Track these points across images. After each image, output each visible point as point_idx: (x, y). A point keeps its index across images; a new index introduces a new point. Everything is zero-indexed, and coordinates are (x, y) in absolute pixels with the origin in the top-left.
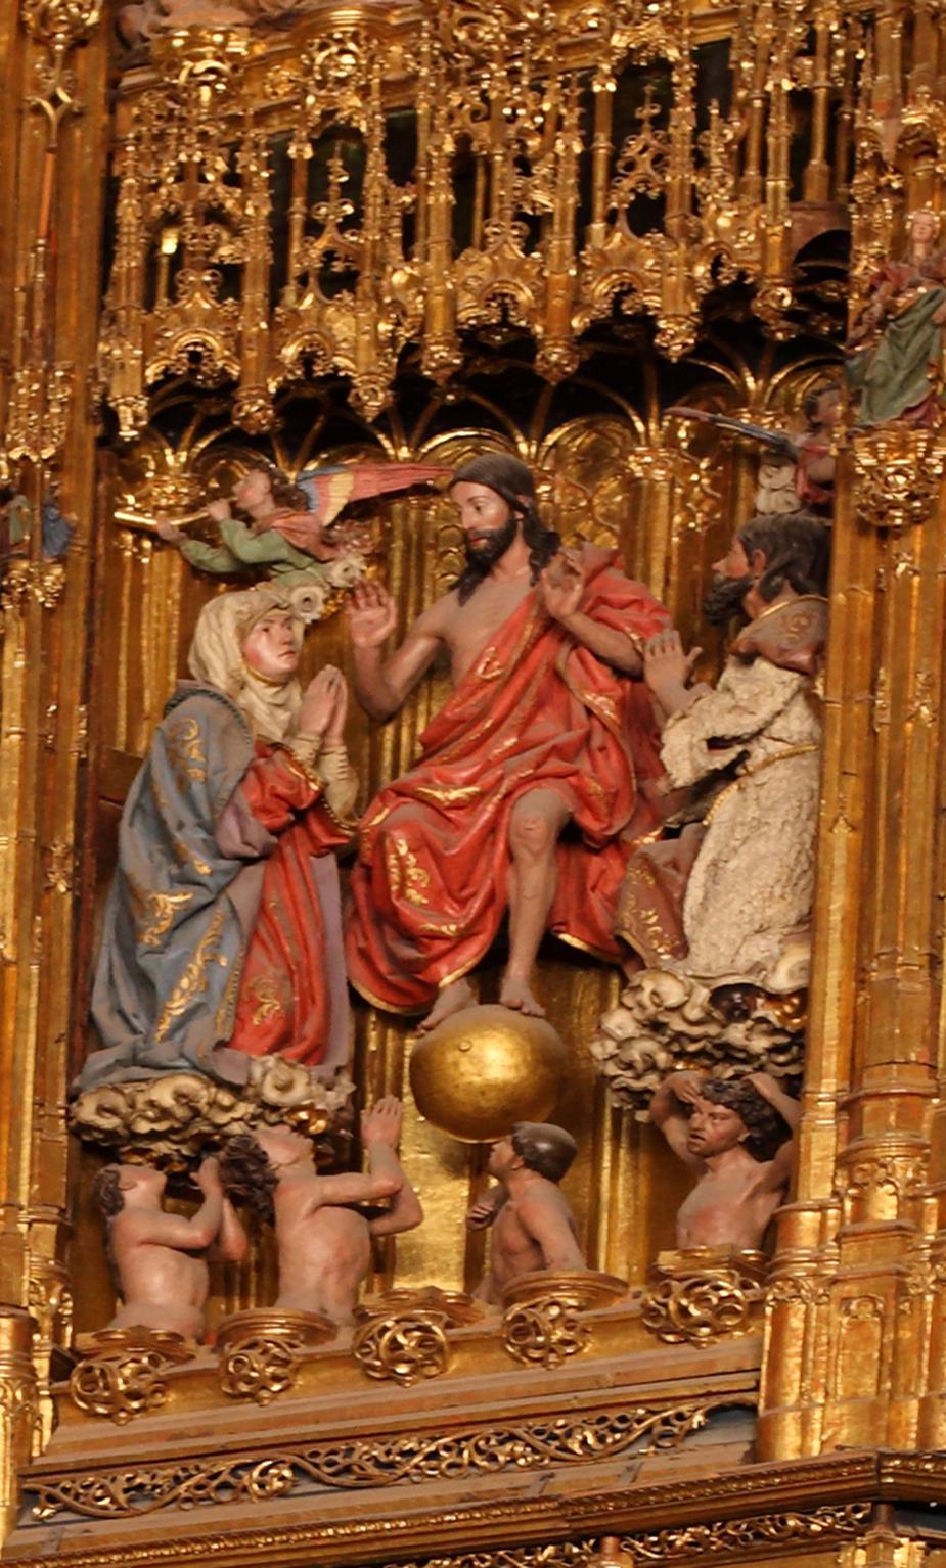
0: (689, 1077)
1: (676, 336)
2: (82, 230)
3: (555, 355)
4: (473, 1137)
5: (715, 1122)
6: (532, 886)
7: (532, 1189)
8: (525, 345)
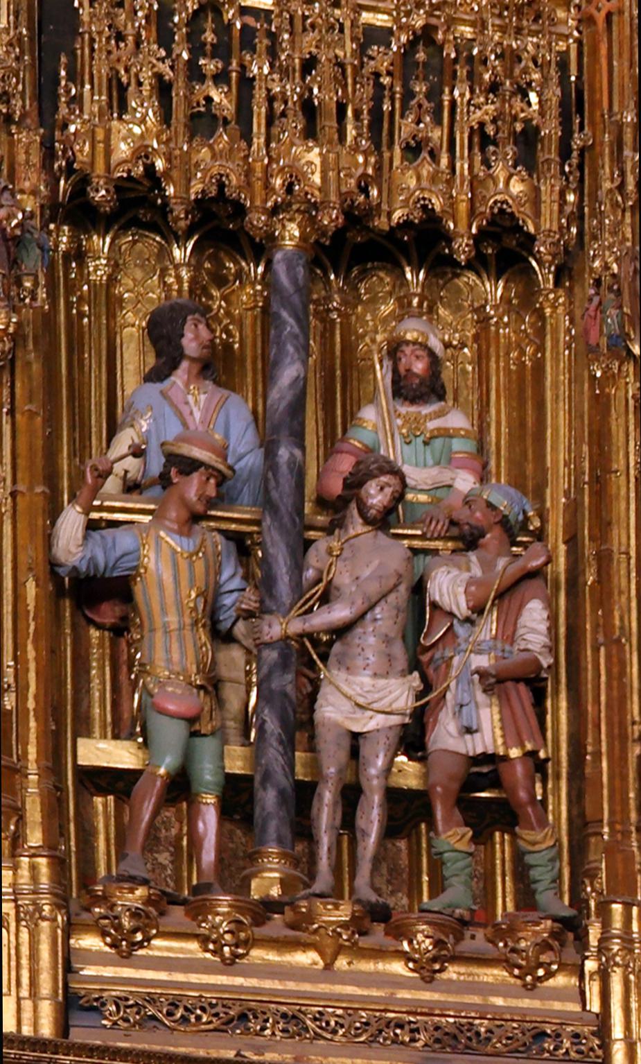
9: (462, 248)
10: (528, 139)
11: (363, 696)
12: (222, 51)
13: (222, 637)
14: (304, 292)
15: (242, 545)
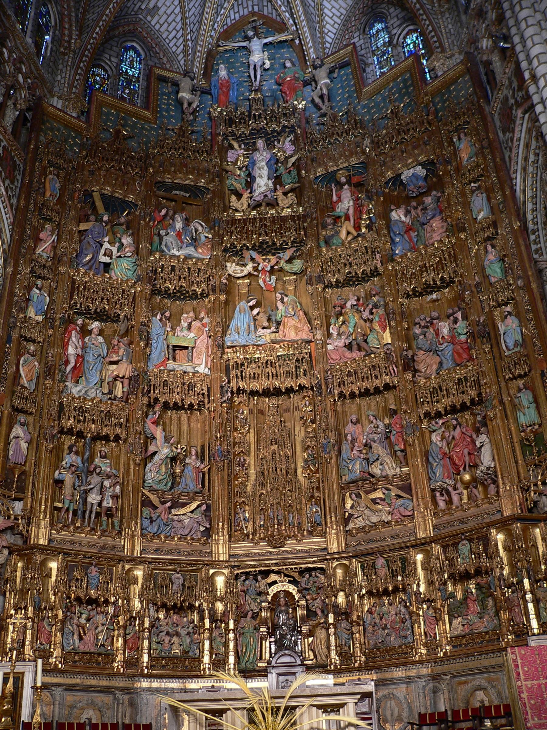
0: (486, 477)
2: (414, 399)
4: (467, 486)
5: (489, 481)
7: (474, 489)
8: (455, 406)
9: (112, 438)
10: (121, 425)
11: (93, 498)
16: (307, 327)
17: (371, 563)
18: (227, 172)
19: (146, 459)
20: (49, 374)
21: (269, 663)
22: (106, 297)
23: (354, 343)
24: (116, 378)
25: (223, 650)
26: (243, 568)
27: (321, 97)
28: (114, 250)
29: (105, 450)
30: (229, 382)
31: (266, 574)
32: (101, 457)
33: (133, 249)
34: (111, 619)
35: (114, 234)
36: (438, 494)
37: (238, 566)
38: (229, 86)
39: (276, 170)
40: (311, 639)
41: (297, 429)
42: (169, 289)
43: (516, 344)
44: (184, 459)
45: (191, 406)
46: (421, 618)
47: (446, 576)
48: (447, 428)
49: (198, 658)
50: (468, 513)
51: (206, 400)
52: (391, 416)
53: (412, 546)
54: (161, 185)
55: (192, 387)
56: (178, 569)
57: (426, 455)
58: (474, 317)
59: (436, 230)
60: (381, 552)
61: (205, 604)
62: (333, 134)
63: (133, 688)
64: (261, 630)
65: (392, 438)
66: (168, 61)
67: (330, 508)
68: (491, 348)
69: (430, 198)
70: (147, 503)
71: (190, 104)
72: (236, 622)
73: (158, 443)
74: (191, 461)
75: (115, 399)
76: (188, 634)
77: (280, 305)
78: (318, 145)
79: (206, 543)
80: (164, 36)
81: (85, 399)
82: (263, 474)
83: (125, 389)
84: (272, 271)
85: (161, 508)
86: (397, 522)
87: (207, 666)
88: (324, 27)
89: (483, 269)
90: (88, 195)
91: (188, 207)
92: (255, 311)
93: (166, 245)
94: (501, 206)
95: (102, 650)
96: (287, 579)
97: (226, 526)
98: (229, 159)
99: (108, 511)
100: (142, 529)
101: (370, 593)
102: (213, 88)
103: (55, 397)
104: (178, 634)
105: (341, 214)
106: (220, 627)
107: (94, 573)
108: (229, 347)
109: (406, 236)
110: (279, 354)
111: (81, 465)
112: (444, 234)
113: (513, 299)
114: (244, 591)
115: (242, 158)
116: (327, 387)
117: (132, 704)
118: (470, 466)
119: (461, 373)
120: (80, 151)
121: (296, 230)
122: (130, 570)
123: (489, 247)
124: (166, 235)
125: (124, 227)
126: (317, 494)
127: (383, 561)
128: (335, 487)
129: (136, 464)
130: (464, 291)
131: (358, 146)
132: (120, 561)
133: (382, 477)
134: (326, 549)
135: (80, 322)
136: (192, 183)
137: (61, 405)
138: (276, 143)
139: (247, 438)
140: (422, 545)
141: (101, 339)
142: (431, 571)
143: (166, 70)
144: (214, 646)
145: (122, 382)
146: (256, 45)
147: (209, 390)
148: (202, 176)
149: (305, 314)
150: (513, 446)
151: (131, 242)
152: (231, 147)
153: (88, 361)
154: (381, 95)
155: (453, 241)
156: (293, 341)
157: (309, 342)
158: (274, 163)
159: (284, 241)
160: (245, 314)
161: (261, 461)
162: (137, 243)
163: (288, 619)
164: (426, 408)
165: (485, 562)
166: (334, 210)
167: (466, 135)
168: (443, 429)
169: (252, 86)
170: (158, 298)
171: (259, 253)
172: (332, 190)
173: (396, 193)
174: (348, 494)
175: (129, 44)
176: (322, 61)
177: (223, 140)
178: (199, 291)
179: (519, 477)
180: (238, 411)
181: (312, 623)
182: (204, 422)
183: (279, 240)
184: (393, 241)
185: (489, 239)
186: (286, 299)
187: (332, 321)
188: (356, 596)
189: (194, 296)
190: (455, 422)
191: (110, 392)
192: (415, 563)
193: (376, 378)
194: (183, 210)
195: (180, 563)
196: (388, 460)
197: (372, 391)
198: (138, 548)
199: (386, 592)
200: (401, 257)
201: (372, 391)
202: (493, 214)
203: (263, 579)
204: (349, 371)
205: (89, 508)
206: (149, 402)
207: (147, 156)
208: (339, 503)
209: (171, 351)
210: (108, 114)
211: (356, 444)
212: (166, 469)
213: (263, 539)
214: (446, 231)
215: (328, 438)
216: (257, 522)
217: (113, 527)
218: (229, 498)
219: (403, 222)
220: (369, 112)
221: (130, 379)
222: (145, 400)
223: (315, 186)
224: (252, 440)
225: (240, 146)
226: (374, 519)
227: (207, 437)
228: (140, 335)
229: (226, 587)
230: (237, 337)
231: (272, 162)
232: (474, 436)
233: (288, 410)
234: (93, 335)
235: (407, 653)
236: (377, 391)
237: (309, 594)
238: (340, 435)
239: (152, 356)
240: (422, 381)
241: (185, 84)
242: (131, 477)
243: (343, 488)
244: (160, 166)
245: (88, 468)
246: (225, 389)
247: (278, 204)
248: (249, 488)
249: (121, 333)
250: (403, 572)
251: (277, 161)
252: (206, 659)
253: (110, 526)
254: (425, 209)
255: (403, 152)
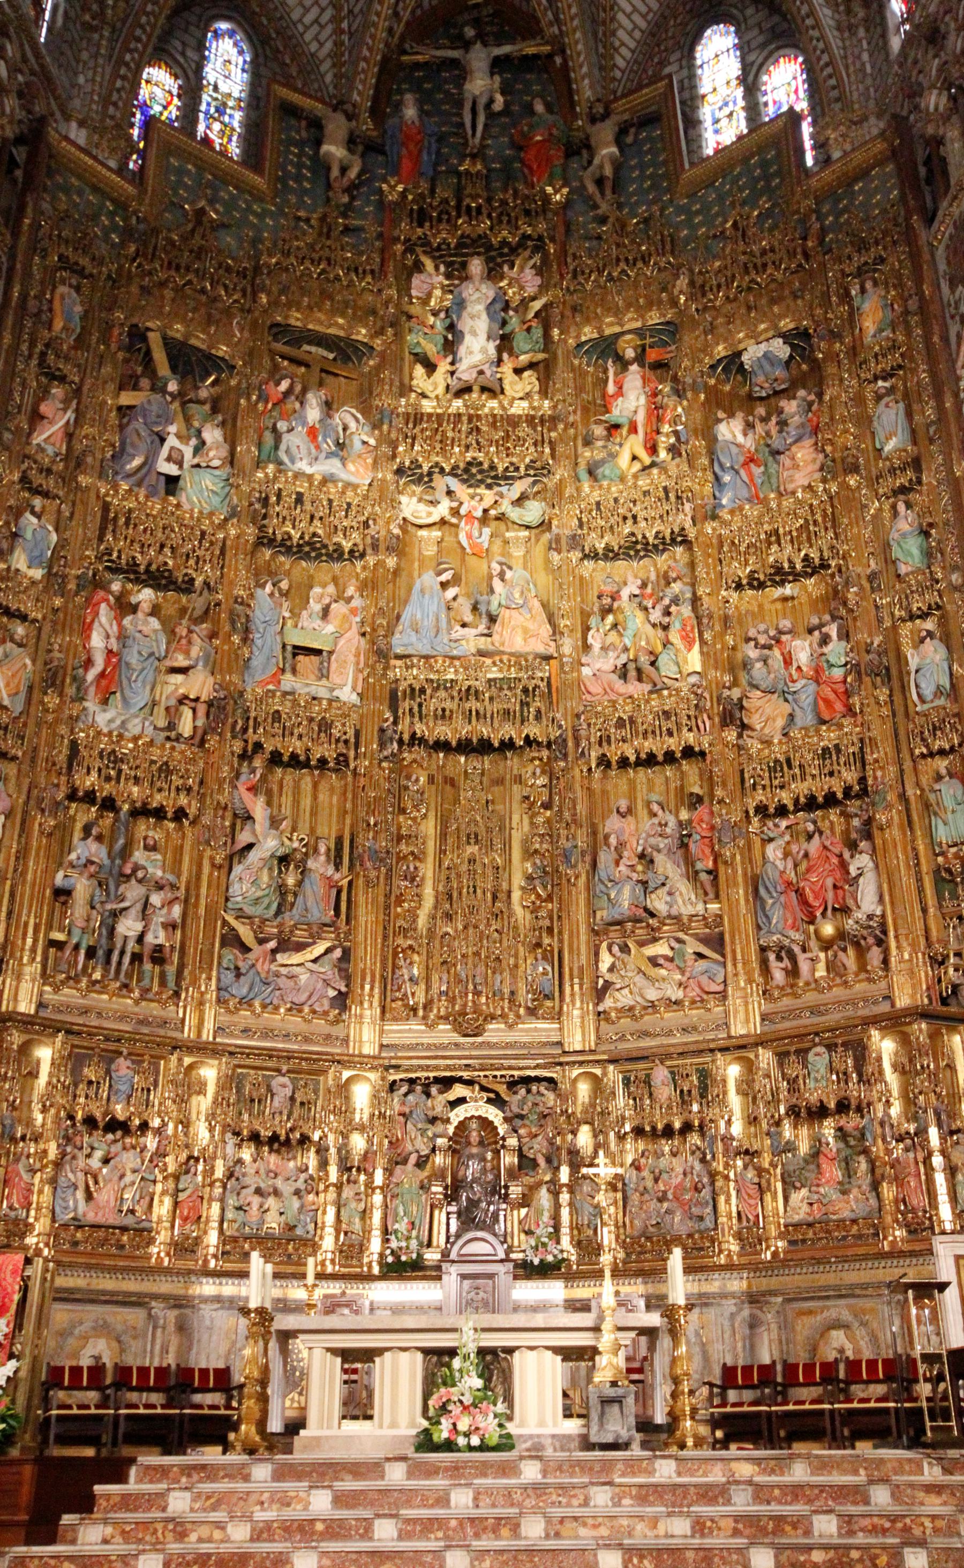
0: (865, 932)
1: (840, 795)
2: (738, 780)
3: (820, 799)
4: (826, 945)
5: (871, 940)
6: (830, 895)
7: (841, 954)
9: (170, 815)
10: (189, 790)
11: (129, 927)
12: (115, 762)
13: (93, 908)
14: (128, 822)
15: (100, 885)
16: (546, 629)
17: (642, 1075)
18: (410, 317)
19: (230, 858)
20: (53, 684)
21: (445, 1254)
22: (169, 543)
23: (631, 666)
24: (183, 700)
25: (357, 1225)
26: (407, 1071)
27: (600, 182)
28: (188, 451)
29: (156, 835)
30: (395, 723)
31: (447, 1083)
32: (146, 848)
33: (224, 452)
34: (151, 1161)
35: (188, 420)
36: (772, 957)
37: (397, 1067)
38: (421, 141)
39: (504, 323)
40: (524, 1211)
41: (516, 818)
42: (290, 538)
43: (939, 692)
44: (304, 861)
45: (323, 762)
46: (732, 1184)
47: (782, 1110)
48: (795, 836)
49: (312, 1240)
50: (828, 996)
51: (352, 754)
52: (692, 807)
53: (722, 1050)
54: (280, 331)
55: (325, 726)
56: (285, 1068)
57: (755, 884)
58: (862, 636)
59: (803, 465)
60: (664, 1057)
61: (331, 1137)
62: (618, 260)
63: (186, 1297)
64: (434, 1189)
65: (692, 847)
66: (300, 72)
67: (571, 970)
68: (890, 696)
69: (794, 403)
70: (232, 940)
71: (344, 170)
72: (389, 1172)
73: (258, 827)
74: (319, 865)
75: (177, 740)
76: (297, 1193)
77: (497, 584)
78: (587, 280)
79: (337, 1021)
80: (295, 16)
81: (120, 736)
82: (450, 897)
83: (200, 723)
84: (485, 519)
85: (257, 950)
86: (693, 1002)
87: (329, 1256)
88: (614, 33)
89: (887, 546)
90: (138, 335)
91: (330, 380)
92: (451, 592)
93: (287, 451)
94: (932, 430)
95: (129, 1221)
96: (485, 1095)
97: (376, 991)
98: (414, 293)
99: (155, 951)
100: (219, 989)
101: (638, 1132)
102: (388, 142)
103: (63, 730)
104: (276, 1193)
105: (623, 420)
106: (355, 1182)
107: (124, 1071)
108: (399, 657)
109: (743, 473)
110: (490, 676)
111: (107, 862)
112: (818, 475)
113: (939, 607)
114: (403, 1115)
115: (438, 292)
116: (577, 745)
117: (182, 1328)
118: (834, 909)
119: (829, 737)
120: (123, 244)
121: (535, 444)
122: (191, 1067)
123: (901, 507)
124: (290, 430)
125: (207, 407)
126: (546, 941)
127: (666, 1072)
128: (583, 929)
129: (213, 865)
130: (847, 584)
131: (664, 289)
132: (175, 1048)
133: (670, 917)
134: (560, 1044)
135: (116, 587)
136: (342, 333)
137: (74, 745)
138: (506, 268)
139: (422, 828)
140: (739, 1048)
141: (154, 623)
142: (754, 1098)
143: (296, 90)
144: (344, 1218)
145: (194, 710)
146: (479, 59)
147: (357, 734)
148: (362, 321)
149: (545, 606)
150: (919, 880)
151: (221, 439)
152: (418, 267)
153: (128, 664)
154: (717, 189)
155: (834, 488)
156: (517, 655)
157: (547, 658)
158: (501, 308)
159: (512, 464)
160: (432, 597)
161: (447, 874)
162: (232, 441)
163: (484, 1171)
164: (760, 796)
165: (855, 1090)
166: (608, 411)
167: (876, 284)
168: (787, 838)
169: (466, 144)
170: (268, 553)
171: (464, 481)
172: (605, 371)
173: (727, 388)
174: (604, 945)
175: (224, 26)
176: (607, 108)
177: (405, 252)
178: (347, 545)
179: (927, 939)
180: (408, 777)
181: (528, 1180)
182: (345, 793)
183: (501, 459)
184: (717, 478)
185: (903, 490)
186: (509, 574)
187: (593, 621)
188: (612, 1134)
189: (337, 554)
190: (811, 827)
191: (171, 726)
192: (724, 1081)
193: (670, 734)
194: (321, 384)
195: (289, 1056)
196: (684, 887)
197: (660, 758)
198: (209, 1026)
199: (668, 1132)
200: (732, 512)
201: (660, 758)
202: (915, 443)
203: (441, 1092)
204: (620, 718)
205: (119, 946)
206: (245, 750)
207: (257, 269)
208: (589, 959)
209: (289, 655)
210: (181, 172)
211: (626, 854)
212: (271, 877)
213: (445, 1018)
214: (821, 469)
215: (574, 837)
216: (435, 986)
217: (163, 983)
218: (385, 938)
219: (738, 445)
220: (689, 223)
221: (210, 704)
222: (238, 746)
223: (576, 362)
224: (431, 831)
225: (437, 268)
226: (652, 994)
227: (348, 821)
228: (233, 623)
229: (372, 1105)
230: (414, 638)
231: (498, 306)
232: (847, 855)
233: (500, 781)
234: (140, 615)
235: (702, 1249)
236: (670, 758)
237: (524, 1126)
238: (595, 833)
239: (254, 663)
240: (754, 746)
241: (337, 126)
242: (204, 891)
243: (596, 933)
244: (282, 292)
245: (120, 867)
246: (389, 733)
247: (502, 392)
248: (422, 921)
249: (198, 613)
250: (702, 1097)
251: (506, 307)
252: (328, 1242)
253: (156, 980)
254: (783, 424)
255: (749, 308)
